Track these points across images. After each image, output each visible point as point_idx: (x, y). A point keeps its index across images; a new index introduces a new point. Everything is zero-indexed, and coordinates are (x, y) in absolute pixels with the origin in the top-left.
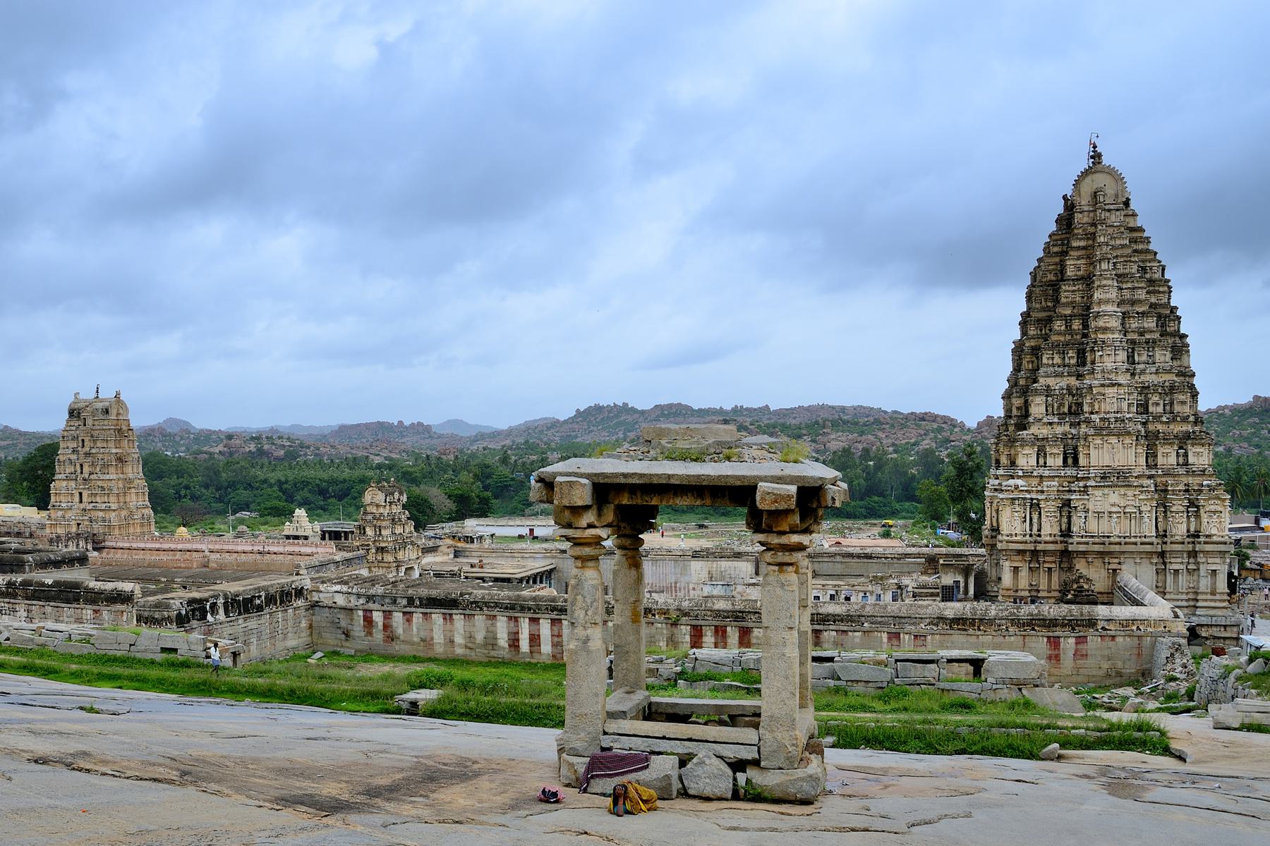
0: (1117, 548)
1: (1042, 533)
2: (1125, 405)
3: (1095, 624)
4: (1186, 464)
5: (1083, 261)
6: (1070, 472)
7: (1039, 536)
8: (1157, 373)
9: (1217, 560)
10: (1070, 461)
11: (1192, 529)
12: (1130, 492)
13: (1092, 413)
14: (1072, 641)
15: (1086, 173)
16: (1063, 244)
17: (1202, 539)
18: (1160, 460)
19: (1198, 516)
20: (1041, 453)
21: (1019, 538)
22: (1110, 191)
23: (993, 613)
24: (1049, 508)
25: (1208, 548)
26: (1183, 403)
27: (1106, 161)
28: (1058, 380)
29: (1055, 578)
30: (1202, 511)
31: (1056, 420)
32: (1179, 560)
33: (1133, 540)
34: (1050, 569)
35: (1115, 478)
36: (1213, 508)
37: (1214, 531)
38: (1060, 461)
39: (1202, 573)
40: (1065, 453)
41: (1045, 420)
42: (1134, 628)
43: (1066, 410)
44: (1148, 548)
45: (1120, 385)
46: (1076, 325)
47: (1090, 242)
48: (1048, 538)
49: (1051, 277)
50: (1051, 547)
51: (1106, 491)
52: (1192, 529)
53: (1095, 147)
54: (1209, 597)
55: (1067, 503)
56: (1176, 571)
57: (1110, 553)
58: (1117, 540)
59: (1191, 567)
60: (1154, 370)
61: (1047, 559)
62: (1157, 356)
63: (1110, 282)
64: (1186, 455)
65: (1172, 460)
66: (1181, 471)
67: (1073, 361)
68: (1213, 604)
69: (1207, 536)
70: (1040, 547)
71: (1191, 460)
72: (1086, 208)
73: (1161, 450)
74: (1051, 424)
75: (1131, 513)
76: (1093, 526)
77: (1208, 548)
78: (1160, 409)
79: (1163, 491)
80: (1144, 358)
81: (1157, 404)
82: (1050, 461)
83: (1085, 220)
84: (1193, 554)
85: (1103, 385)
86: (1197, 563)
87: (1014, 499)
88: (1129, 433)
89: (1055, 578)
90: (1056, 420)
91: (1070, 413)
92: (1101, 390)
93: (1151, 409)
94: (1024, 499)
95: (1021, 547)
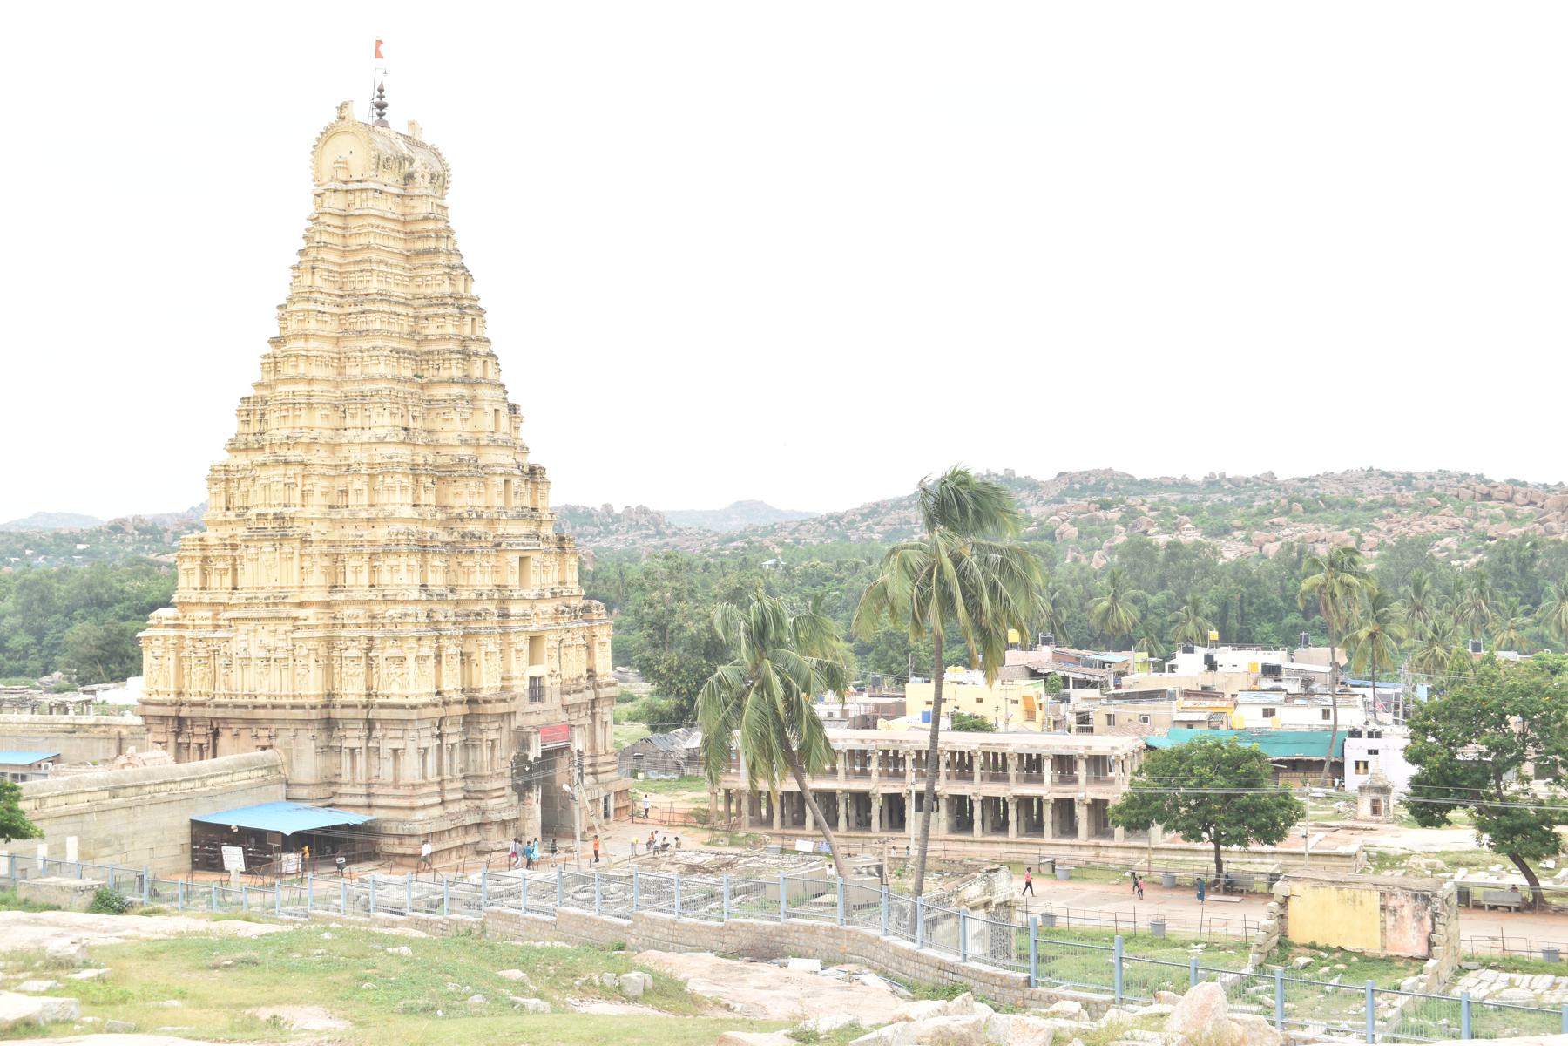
0: (260, 713)
15: (327, 135)
18: (350, 579)
25: (384, 714)
32: (356, 733)
37: (395, 689)
51: (253, 624)
53: (381, 90)
54: (391, 791)
56: (352, 750)
57: (255, 721)
61: (197, 730)
65: (364, 579)
68: (393, 802)
70: (185, 712)
73: (352, 563)
80: (358, 422)
84: (370, 724)
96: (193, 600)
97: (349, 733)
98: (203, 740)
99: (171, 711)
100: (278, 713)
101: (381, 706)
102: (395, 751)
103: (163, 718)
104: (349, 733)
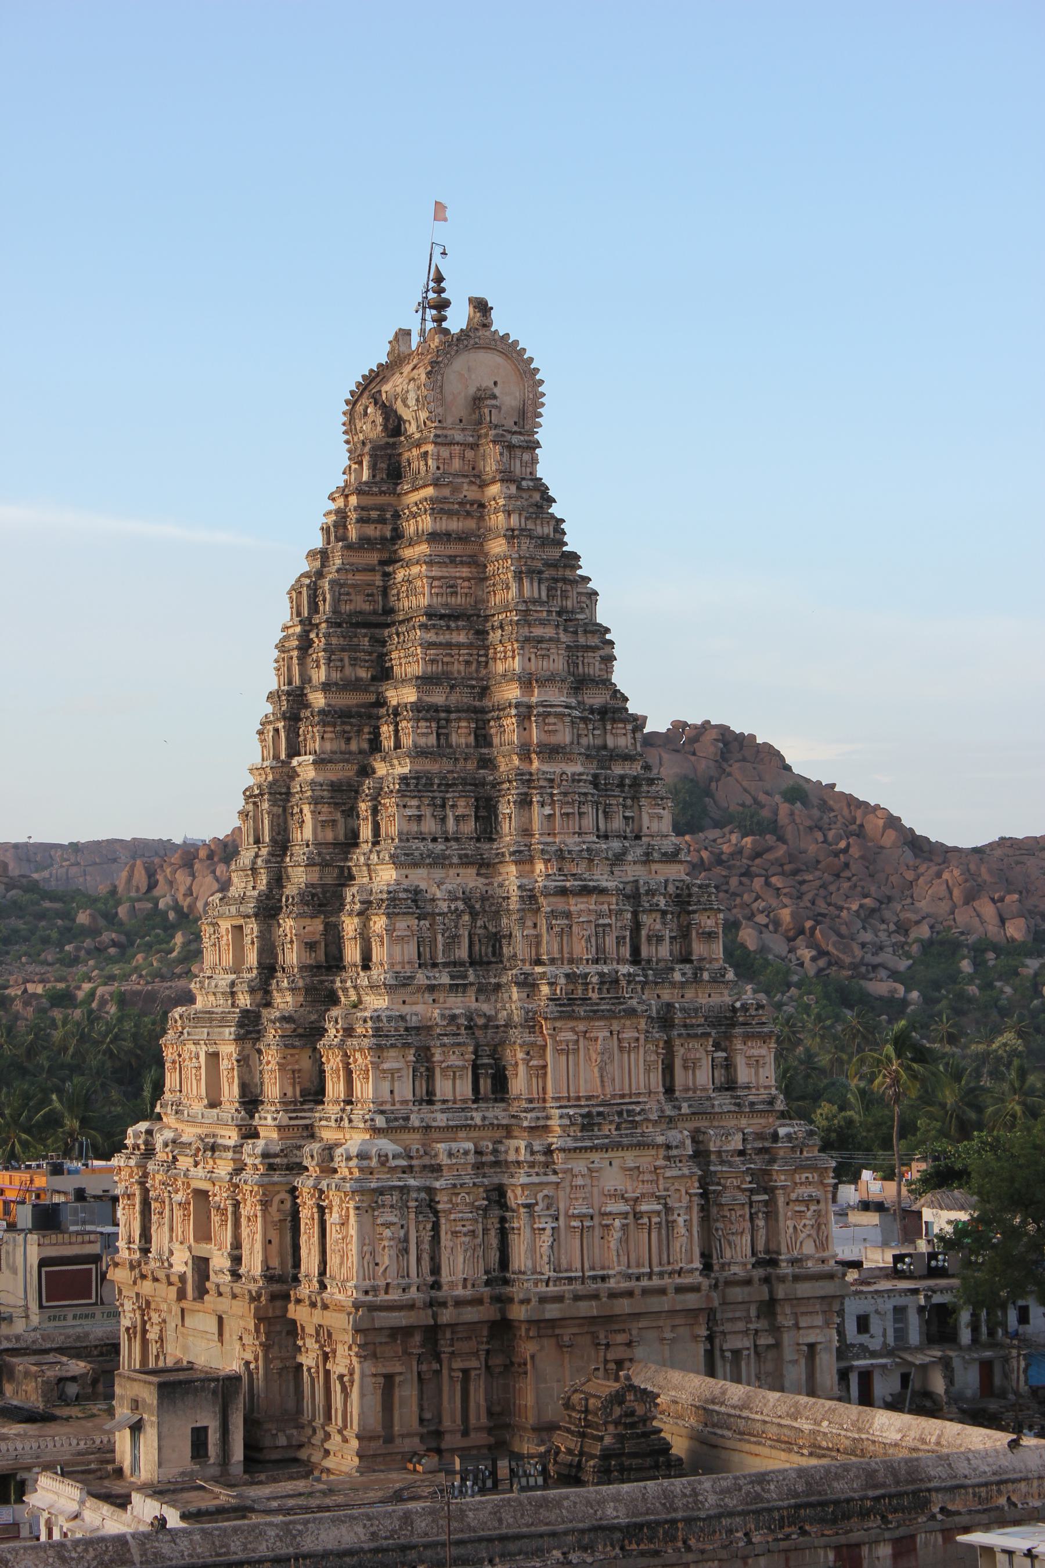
0: (624, 1306)
1: (445, 1277)
2: (610, 942)
3: (926, 1503)
4: (729, 1086)
5: (465, 571)
6: (497, 1113)
7: (436, 1285)
8: (647, 859)
9: (819, 1320)
10: (486, 1085)
11: (760, 1246)
12: (646, 1160)
13: (539, 962)
14: (885, 1551)
16: (382, 521)
17: (785, 1269)
18: (680, 1077)
19: (771, 1215)
20: (424, 1067)
21: (394, 1296)
22: (509, 397)
23: (712, 1499)
24: (459, 1214)
26: (709, 936)
27: (500, 323)
28: (438, 873)
29: (478, 1396)
30: (781, 1201)
31: (446, 980)
32: (740, 1326)
33: (656, 1282)
34: (466, 1372)
35: (601, 1124)
36: (804, 1191)
37: (809, 1248)
38: (465, 1088)
39: (789, 1354)
40: (475, 1067)
41: (421, 978)
42: (1002, 1501)
43: (462, 953)
44: (692, 1300)
45: (602, 891)
46: (461, 736)
47: (471, 524)
48: (459, 1292)
49: (359, 603)
50: (470, 1314)
52: (760, 1246)
53: (439, 279)
55: (498, 1196)
56: (736, 1353)
57: (609, 1319)
58: (625, 1285)
59: (765, 1340)
60: (639, 851)
61: (458, 1345)
62: (646, 821)
63: (549, 632)
64: (729, 1065)
65: (703, 1077)
66: (722, 1102)
67: (469, 827)
69: (793, 1262)
70: (447, 1316)
71: (743, 1075)
72: (459, 437)
74: (432, 988)
75: (650, 1214)
76: (572, 1252)
77: (804, 1289)
78: (664, 951)
79: (701, 1155)
81: (660, 939)
82: (443, 1087)
83: (457, 464)
84: (769, 1308)
85: (563, 892)
86: (776, 1330)
87: (381, 1191)
88: (632, 1013)
89: (478, 1396)
90: (446, 980)
91: (474, 962)
92: (560, 903)
93: (644, 953)
94: (404, 1190)
95: (400, 1319)
96: (417, 1124)
97: (728, 1327)
98: (474, 1363)
99: (425, 1318)
100: (656, 1304)
101: (797, 1278)
102: (812, 1346)
103: (406, 1332)
104: (728, 1327)
